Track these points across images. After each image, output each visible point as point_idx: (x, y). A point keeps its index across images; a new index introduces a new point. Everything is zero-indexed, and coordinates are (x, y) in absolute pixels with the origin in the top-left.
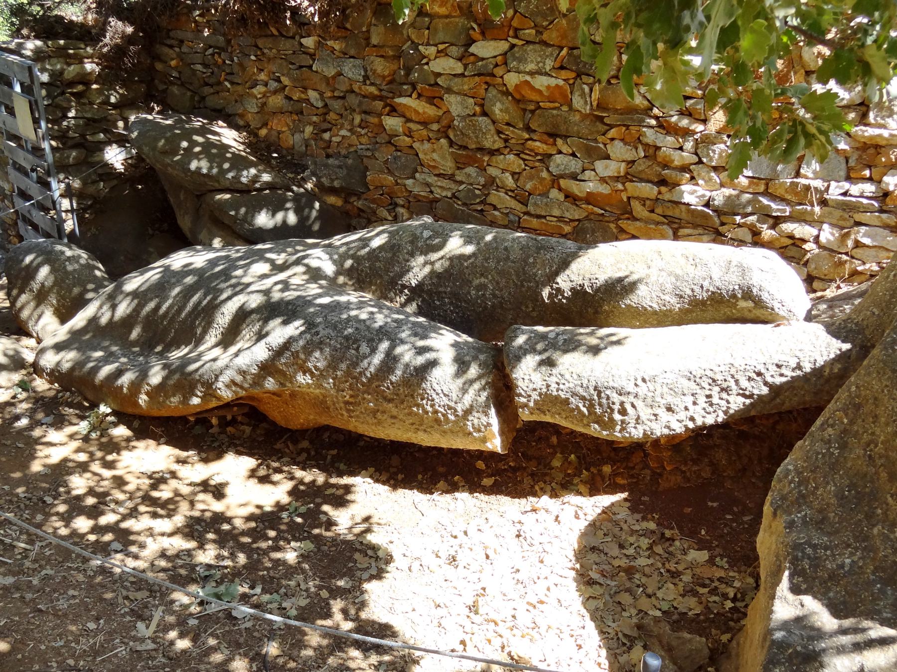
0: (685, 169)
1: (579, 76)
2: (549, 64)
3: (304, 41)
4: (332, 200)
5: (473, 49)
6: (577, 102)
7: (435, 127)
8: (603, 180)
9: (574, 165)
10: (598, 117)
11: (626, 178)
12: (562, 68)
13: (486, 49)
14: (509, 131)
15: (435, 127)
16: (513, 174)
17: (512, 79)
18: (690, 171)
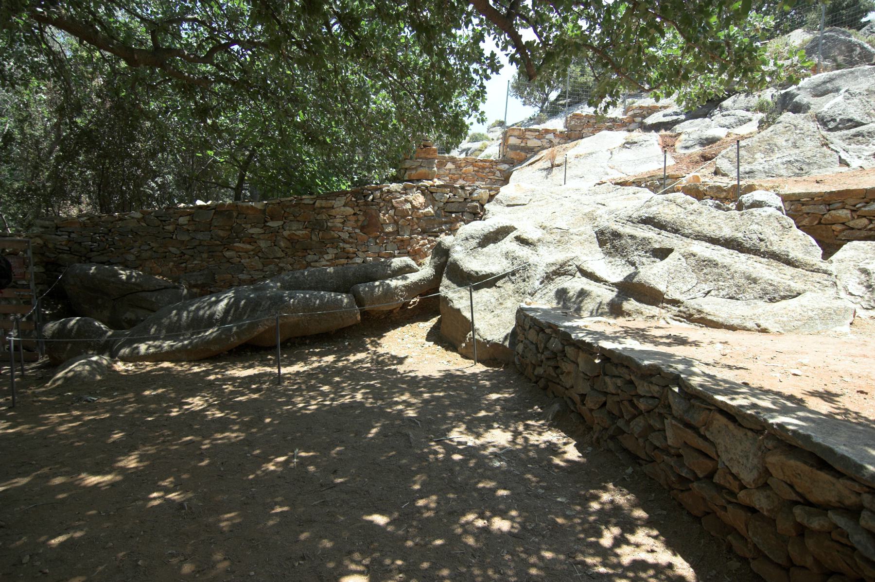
1: (313, 229)
2: (301, 227)
3: (166, 228)
5: (268, 224)
6: (314, 237)
7: (252, 253)
8: (328, 261)
9: (316, 258)
10: (322, 242)
11: (336, 258)
14: (287, 250)
15: (252, 253)
17: (286, 233)
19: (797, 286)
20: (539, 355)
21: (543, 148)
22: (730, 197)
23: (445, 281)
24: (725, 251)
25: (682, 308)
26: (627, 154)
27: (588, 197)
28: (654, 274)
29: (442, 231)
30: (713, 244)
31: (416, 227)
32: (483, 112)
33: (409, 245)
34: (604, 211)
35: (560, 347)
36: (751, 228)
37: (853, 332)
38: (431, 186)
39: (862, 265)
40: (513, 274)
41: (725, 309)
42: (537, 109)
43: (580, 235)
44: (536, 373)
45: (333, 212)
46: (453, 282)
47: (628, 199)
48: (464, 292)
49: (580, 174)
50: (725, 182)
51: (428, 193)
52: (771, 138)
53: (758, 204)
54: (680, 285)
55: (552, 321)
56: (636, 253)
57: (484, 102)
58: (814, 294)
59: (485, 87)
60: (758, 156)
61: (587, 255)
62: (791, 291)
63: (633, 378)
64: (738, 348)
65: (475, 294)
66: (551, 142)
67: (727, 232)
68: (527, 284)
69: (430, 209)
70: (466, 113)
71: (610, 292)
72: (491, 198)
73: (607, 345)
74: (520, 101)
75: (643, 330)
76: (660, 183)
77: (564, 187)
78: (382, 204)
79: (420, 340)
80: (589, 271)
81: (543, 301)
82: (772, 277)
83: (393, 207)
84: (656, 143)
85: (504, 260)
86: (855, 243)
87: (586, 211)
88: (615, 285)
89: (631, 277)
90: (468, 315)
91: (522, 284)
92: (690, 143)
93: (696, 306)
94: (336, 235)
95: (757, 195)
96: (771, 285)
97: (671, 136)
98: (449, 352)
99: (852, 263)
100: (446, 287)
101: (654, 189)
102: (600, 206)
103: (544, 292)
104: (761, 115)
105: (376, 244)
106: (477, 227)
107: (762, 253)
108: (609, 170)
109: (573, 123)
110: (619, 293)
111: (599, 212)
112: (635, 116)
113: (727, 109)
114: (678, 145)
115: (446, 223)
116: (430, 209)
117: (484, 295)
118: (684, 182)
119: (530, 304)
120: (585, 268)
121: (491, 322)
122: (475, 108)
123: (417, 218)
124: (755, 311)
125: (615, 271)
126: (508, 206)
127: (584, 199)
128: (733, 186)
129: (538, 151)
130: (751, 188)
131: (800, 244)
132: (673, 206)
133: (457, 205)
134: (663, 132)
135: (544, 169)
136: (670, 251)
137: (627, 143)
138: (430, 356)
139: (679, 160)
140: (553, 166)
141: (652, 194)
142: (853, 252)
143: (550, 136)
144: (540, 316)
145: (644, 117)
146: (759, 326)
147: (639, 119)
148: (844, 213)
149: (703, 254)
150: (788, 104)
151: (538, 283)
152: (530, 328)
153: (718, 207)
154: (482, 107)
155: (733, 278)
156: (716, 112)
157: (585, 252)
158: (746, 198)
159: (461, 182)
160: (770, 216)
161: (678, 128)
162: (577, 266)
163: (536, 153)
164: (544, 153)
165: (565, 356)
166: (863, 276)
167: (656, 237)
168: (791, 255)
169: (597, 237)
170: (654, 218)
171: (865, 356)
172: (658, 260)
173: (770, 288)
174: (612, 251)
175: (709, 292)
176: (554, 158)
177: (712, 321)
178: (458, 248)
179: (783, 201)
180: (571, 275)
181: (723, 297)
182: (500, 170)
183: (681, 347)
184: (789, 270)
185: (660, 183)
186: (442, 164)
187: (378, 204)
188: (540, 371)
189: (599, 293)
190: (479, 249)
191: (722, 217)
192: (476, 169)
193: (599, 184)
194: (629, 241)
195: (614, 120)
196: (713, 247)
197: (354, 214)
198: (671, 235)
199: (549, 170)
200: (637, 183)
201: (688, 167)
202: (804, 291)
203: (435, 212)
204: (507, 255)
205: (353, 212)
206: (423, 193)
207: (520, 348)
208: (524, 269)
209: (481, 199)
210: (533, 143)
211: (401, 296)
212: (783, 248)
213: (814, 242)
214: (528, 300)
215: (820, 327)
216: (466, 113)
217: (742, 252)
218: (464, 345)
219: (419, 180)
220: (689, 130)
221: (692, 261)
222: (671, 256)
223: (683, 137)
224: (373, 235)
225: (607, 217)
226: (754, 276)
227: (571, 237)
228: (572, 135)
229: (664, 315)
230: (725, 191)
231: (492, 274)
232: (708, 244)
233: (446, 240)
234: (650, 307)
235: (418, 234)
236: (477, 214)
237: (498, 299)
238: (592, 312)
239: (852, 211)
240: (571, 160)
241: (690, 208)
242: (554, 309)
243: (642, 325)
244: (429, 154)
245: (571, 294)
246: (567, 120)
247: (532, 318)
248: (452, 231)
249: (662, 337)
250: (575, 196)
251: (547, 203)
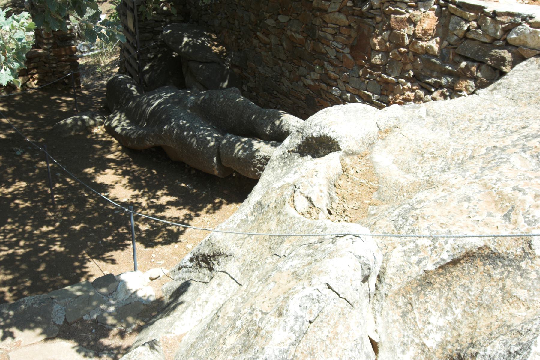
0: (335, 80)
2: (300, 30)
4: (236, 70)
12: (303, 32)
13: (283, 19)
16: (289, 72)
18: (337, 82)
31: (409, 66)
45: (327, 17)
78: (378, 19)
83: (390, 28)
94: (323, 50)
115: (450, 74)
133: (476, 47)
197: (350, 26)
203: (440, 50)
205: (347, 23)
235: (408, 79)
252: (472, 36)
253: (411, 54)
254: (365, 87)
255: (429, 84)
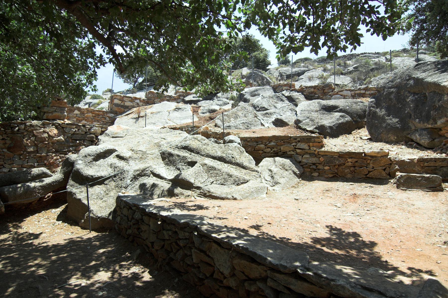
19: (247, 178)
20: (129, 223)
21: (134, 107)
22: (220, 138)
23: (71, 182)
24: (219, 163)
25: (201, 191)
26: (177, 114)
27: (157, 134)
28: (189, 174)
29: (70, 151)
30: (214, 159)
31: (51, 148)
32: (95, 86)
33: (46, 159)
34: (164, 142)
35: (140, 216)
36: (229, 152)
37: (267, 197)
38: (62, 124)
39: (269, 168)
40: (115, 176)
41: (219, 190)
42: (131, 86)
43: (152, 154)
44: (127, 233)
46: (77, 183)
47: (177, 137)
48: (84, 189)
49: (153, 122)
50: (219, 130)
51: (60, 128)
52: (236, 112)
53: (231, 141)
54: (200, 179)
55: (136, 203)
56: (180, 164)
57: (96, 81)
58: (253, 181)
59: (96, 73)
60: (232, 119)
61: (156, 165)
62: (245, 180)
63: (177, 230)
64: (224, 208)
65: (90, 189)
66: (138, 104)
67: (219, 154)
68: (123, 182)
69: (61, 138)
70: (84, 85)
71: (168, 184)
72: (102, 133)
73: (164, 213)
74: (121, 80)
75: (184, 203)
76: (191, 129)
77: (145, 128)
78: (25, 133)
79: (52, 221)
80: (157, 173)
81: (132, 191)
82: (237, 174)
83: (34, 135)
84: (190, 110)
85: (109, 168)
86: (267, 158)
87: (156, 142)
88: (170, 180)
89: (178, 176)
90: (86, 202)
91: (120, 182)
92: (205, 111)
93: (207, 189)
95: (231, 137)
96: (237, 178)
97: (196, 107)
98: (73, 227)
99: (266, 167)
100: (71, 186)
101: (188, 132)
102: (163, 139)
103: (133, 186)
104: (232, 102)
105: (20, 159)
106: (92, 149)
107: (234, 163)
108: (168, 121)
109: (150, 96)
110: (172, 184)
111: (162, 143)
112: (180, 96)
113: (219, 98)
114: (200, 111)
115: (72, 146)
116: (61, 138)
117: (97, 189)
118: (202, 129)
119: (124, 193)
120: (155, 172)
121: (101, 205)
122: (91, 83)
123: (52, 143)
124: (231, 190)
125: (169, 173)
126: (113, 137)
127: (155, 135)
128: (222, 132)
129: (131, 108)
130: (229, 134)
131: (247, 159)
132: (196, 141)
134: (193, 105)
135: (134, 118)
136: (196, 163)
137: (177, 108)
138: (59, 231)
139: (200, 118)
140: (139, 117)
141: (187, 135)
142: (267, 162)
143: (138, 101)
144: (130, 200)
145: (185, 97)
146: (233, 197)
147: (182, 98)
148: (262, 146)
149: (210, 164)
150: (241, 98)
151: (129, 181)
152: (124, 207)
153: (216, 142)
154: (94, 83)
155: (222, 175)
156: (215, 98)
157: (155, 163)
158: (227, 138)
159: (84, 122)
160: (235, 147)
161: (200, 104)
162: (151, 171)
163: (130, 109)
164: (135, 109)
165: (143, 222)
166: (270, 172)
167: (189, 156)
168: (244, 164)
169: (161, 156)
170: (188, 147)
171: (271, 207)
172: (190, 167)
173: (237, 179)
174: (169, 163)
175: (213, 182)
176: (139, 113)
177: (214, 196)
178: (80, 162)
179: (241, 140)
180: (148, 176)
181: (219, 184)
182: (109, 117)
183: (200, 211)
184: (244, 171)
185: (191, 129)
186: (71, 111)
187: (23, 133)
188: (129, 231)
189: (163, 185)
190: (94, 162)
191: (217, 147)
192: (93, 115)
193: (163, 128)
194: (177, 158)
195: (170, 97)
196: (214, 161)
197: (3, 139)
198: (196, 155)
199: (137, 119)
200: (181, 129)
201: (204, 122)
202: (250, 180)
203: (65, 139)
204: (111, 166)
206: (57, 128)
207: (118, 219)
208: (121, 173)
209: (96, 133)
210: (128, 104)
211: (38, 193)
212: (241, 161)
213: (252, 159)
214: (123, 191)
215: (256, 196)
216: (84, 85)
217: (226, 163)
218: (83, 221)
219: (54, 120)
220: (204, 105)
221: (205, 167)
222: (196, 165)
223: (201, 108)
224: (18, 153)
225: (166, 145)
226: (230, 174)
227: (148, 155)
228: (149, 101)
229: (194, 195)
230: (218, 134)
231: (102, 177)
232: (212, 159)
233: (72, 156)
234: (187, 191)
235: (53, 153)
236: (94, 141)
237: (105, 192)
238: (159, 196)
239: (265, 145)
240: (149, 114)
241: (204, 142)
242: (138, 195)
243: (183, 201)
244: (61, 104)
245: (148, 186)
246: (146, 94)
247: (125, 202)
248: (77, 151)
249: (192, 206)
250: (150, 134)
251: (135, 137)
252: (77, 133)
253: (50, 144)
254: (26, 162)
255: (65, 152)
